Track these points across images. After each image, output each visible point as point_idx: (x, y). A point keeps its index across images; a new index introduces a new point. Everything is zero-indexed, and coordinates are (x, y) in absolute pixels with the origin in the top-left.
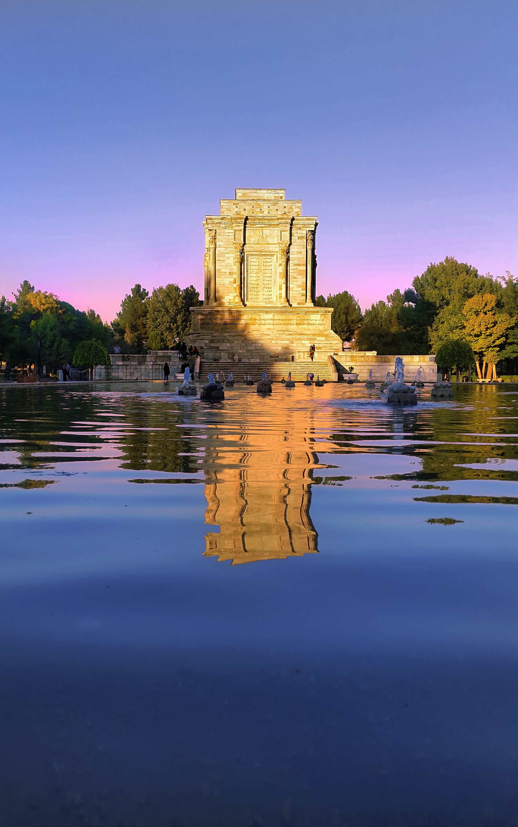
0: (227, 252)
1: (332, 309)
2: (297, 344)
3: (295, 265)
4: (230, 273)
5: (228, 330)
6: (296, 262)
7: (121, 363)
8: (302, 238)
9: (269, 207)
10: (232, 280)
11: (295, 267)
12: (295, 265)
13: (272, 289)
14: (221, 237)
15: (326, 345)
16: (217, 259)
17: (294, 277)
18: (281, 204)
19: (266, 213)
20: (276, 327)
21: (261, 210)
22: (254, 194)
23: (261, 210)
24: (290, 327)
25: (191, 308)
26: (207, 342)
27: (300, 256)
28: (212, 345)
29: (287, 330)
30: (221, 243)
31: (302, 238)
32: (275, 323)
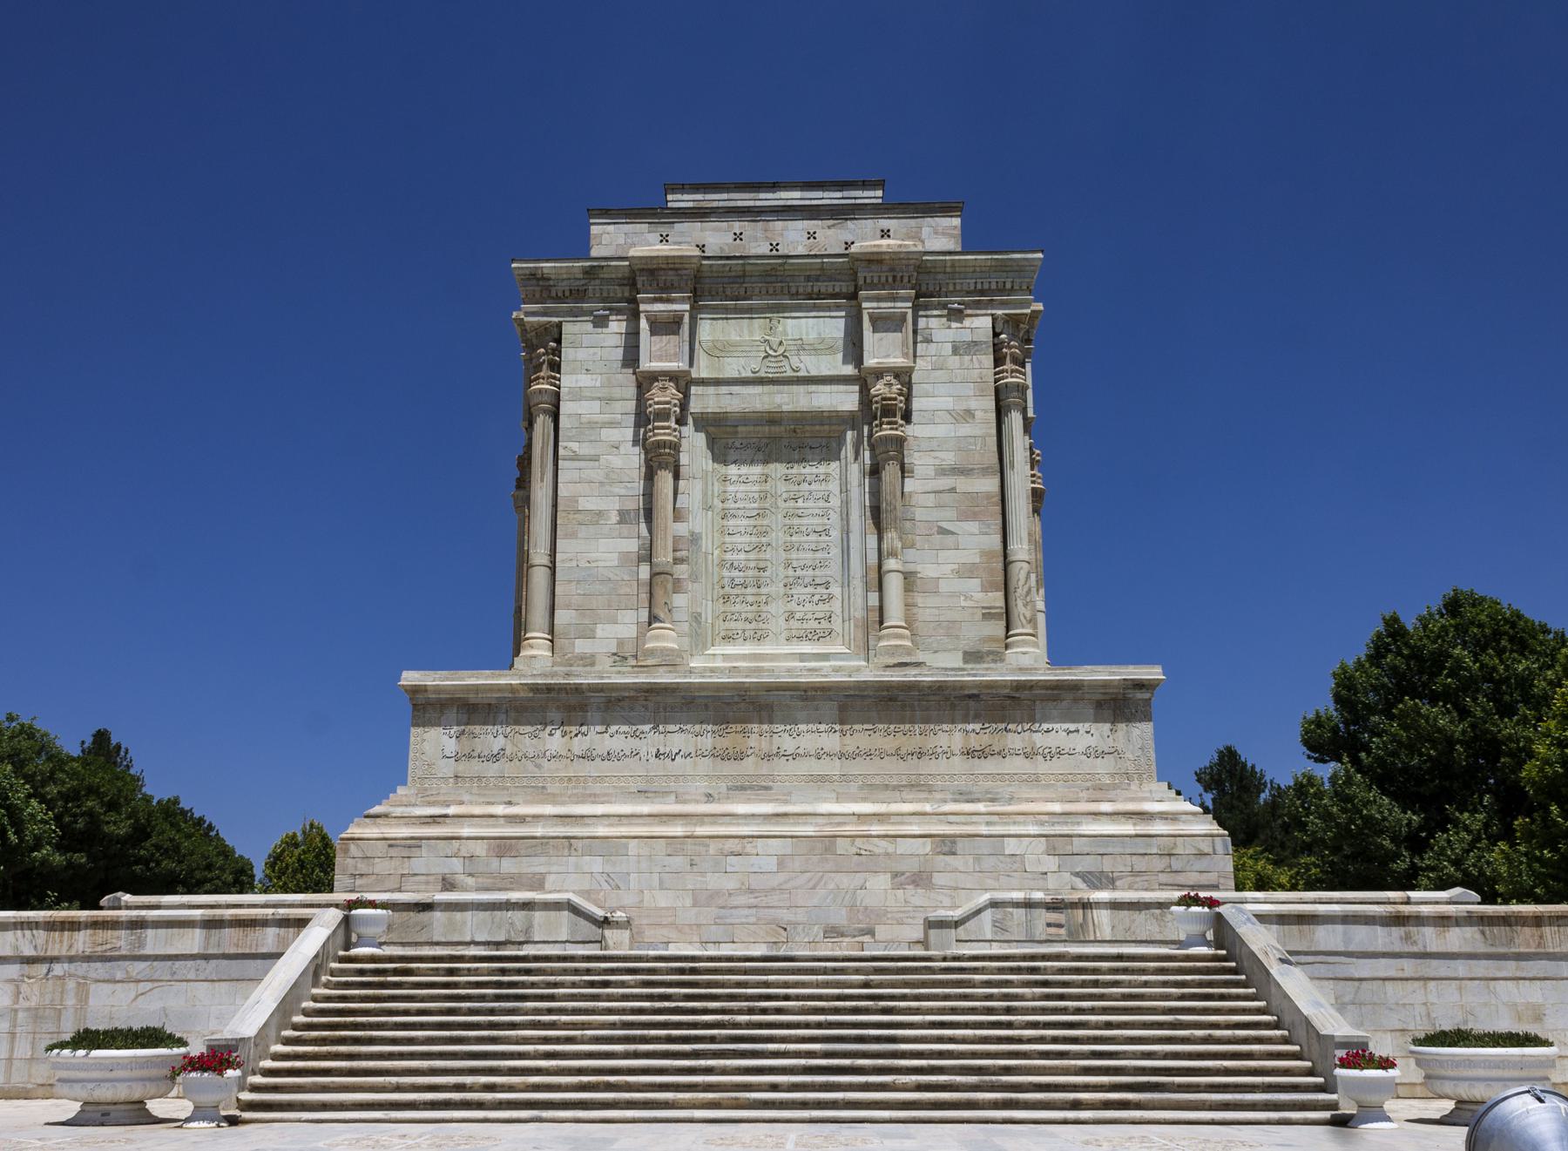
0: (606, 417)
2: (978, 858)
3: (942, 472)
4: (624, 517)
5: (597, 788)
6: (949, 458)
8: (971, 347)
9: (812, 235)
10: (632, 546)
11: (945, 482)
12: (942, 472)
13: (835, 590)
14: (581, 354)
15: (1140, 863)
16: (561, 452)
17: (943, 531)
20: (857, 767)
21: (774, 247)
23: (774, 247)
24: (928, 767)
26: (480, 849)
27: (965, 430)
28: (508, 866)
30: (584, 380)
31: (971, 347)
32: (851, 749)
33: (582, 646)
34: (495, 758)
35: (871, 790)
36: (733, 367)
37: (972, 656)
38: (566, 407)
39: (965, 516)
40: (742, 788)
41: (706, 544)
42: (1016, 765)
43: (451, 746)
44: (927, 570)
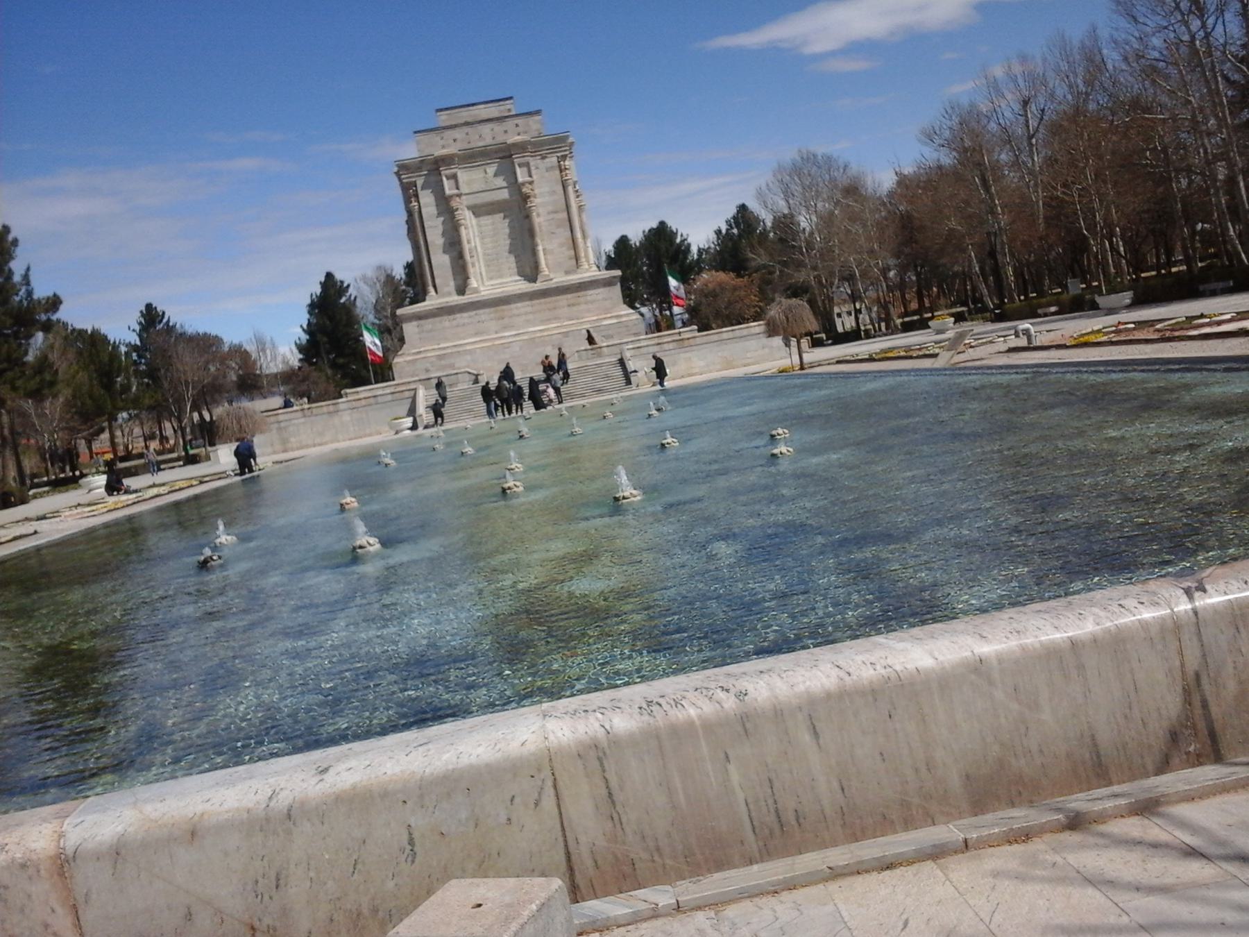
1: (618, 273)
6: (550, 208)
7: (303, 420)
10: (455, 254)
11: (551, 216)
18: (510, 124)
19: (489, 141)
22: (464, 114)
25: (399, 312)
28: (443, 362)
29: (557, 318)
33: (446, 289)
34: (431, 331)
35: (543, 322)
36: (476, 187)
37: (567, 273)
38: (424, 211)
39: (558, 227)
40: (505, 328)
41: (479, 249)
42: (583, 307)
43: (416, 330)
44: (548, 247)
